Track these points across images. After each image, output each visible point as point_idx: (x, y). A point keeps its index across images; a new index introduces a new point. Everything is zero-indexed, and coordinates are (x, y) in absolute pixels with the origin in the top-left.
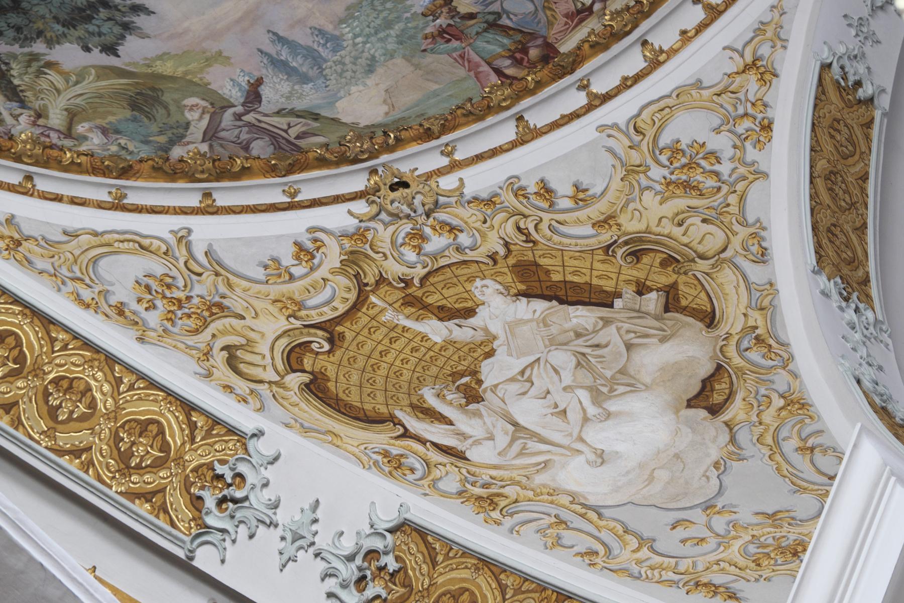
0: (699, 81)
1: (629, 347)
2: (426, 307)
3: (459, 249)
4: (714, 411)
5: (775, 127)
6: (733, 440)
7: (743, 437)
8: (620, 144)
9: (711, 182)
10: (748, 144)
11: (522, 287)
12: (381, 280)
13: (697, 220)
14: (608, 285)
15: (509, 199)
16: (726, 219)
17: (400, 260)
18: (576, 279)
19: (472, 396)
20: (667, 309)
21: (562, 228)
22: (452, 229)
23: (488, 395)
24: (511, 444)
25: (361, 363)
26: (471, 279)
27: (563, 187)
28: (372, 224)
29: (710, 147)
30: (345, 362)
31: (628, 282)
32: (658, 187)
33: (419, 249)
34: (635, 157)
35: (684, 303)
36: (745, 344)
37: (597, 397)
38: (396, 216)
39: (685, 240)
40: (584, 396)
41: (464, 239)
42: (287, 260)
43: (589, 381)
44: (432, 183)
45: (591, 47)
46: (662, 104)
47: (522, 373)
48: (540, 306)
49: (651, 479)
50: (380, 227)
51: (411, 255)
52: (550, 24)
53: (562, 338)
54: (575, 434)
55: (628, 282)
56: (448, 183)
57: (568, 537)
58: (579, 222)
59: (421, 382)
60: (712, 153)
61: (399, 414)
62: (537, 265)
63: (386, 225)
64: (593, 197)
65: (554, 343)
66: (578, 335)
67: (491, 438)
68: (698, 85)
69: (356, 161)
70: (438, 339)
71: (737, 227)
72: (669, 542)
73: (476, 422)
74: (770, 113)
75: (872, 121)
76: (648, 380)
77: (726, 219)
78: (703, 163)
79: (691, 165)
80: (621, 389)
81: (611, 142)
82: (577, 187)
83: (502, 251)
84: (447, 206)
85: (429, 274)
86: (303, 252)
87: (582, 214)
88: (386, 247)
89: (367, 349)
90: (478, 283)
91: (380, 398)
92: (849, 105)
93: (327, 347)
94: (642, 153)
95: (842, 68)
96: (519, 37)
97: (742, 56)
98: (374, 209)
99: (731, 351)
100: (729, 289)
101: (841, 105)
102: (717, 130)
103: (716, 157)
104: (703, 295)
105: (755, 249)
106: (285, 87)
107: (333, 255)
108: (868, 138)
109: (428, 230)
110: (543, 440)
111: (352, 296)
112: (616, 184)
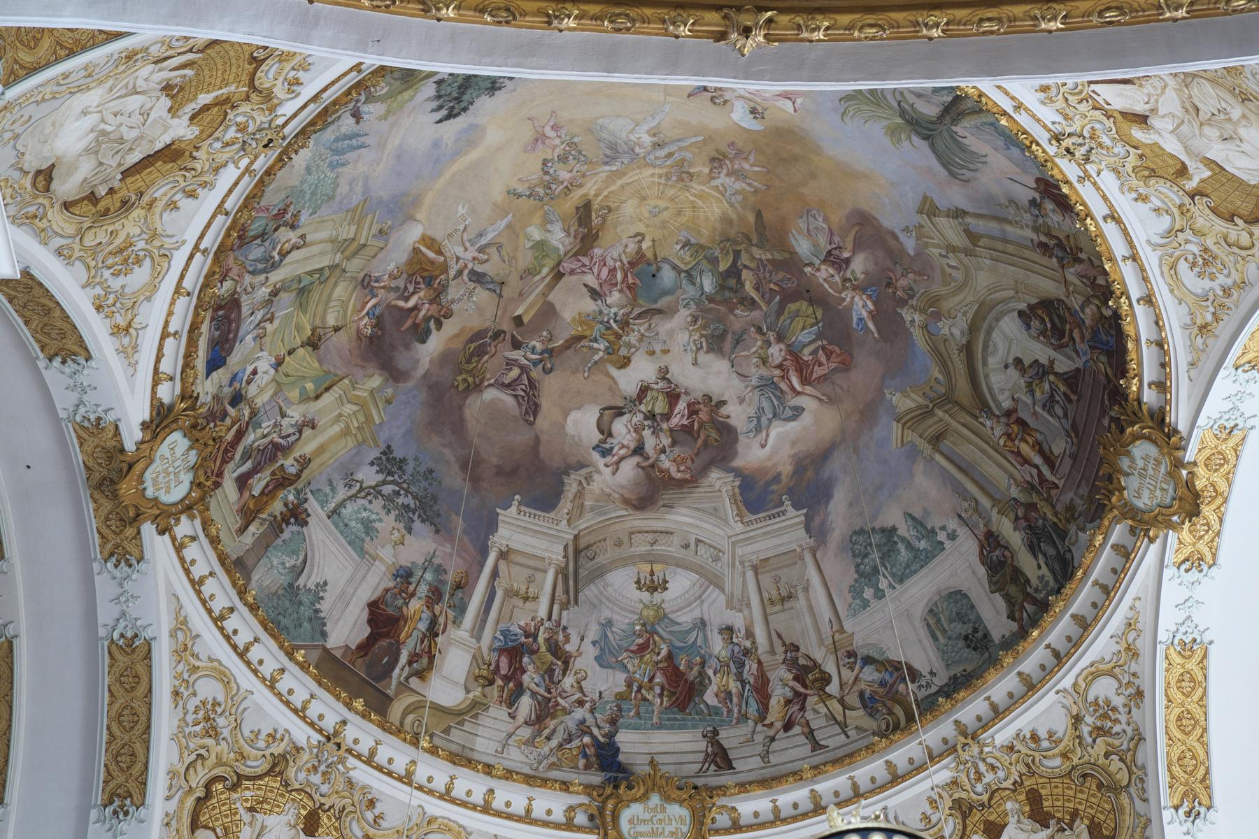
0: (149, 301)
1: (101, 164)
2: (216, 105)
3: (218, 139)
4: (39, 172)
5: (95, 311)
6: (21, 169)
7: (17, 174)
8: (168, 243)
9: (110, 262)
10: (103, 293)
11: (173, 147)
12: (247, 99)
13: (104, 241)
14: (129, 180)
15: (207, 178)
16: (89, 253)
17: (244, 114)
18: (148, 170)
19: (167, 88)
20: (92, 193)
21: (172, 185)
22: (227, 145)
23: (159, 94)
24: (134, 84)
25: (233, 61)
26: (202, 132)
27: (185, 203)
28: (270, 118)
29: (122, 277)
30: (242, 56)
31: (121, 189)
32: (135, 239)
33: (237, 124)
34: (157, 243)
35: (85, 202)
36: (41, 210)
37: (104, 133)
38: (260, 130)
39: (104, 228)
40: (109, 128)
41: (218, 145)
42: (301, 75)
43: (111, 137)
44: (252, 157)
45: (214, 272)
46: (161, 276)
47: (148, 115)
48: (159, 146)
49: (53, 124)
50: (264, 120)
51: (240, 119)
52: (236, 259)
53: (138, 142)
54: (104, 112)
55: (121, 189)
56: (244, 163)
57: (83, 73)
58: (165, 194)
59: (197, 74)
60: (118, 275)
61: (200, 55)
62: (174, 161)
63: (262, 123)
64: (165, 211)
65: (142, 137)
66: (131, 149)
67: (146, 80)
68: (148, 299)
69: (296, 136)
70: (200, 96)
71: (82, 253)
72: (31, 110)
73: (158, 80)
74: (102, 315)
75: (42, 351)
76: (81, 158)
77: (89, 253)
78: (120, 267)
79: (126, 260)
80: (93, 145)
81: (174, 240)
82: (177, 208)
83: (195, 154)
84: (238, 152)
85: (225, 119)
86: (298, 82)
87: (165, 199)
88: (255, 114)
89: (234, 69)
90: (197, 133)
91: (214, 55)
92: (61, 349)
93: (255, 54)
94: (155, 248)
95: (79, 364)
96: (247, 241)
97: (136, 329)
98: (273, 125)
99: (46, 202)
100: (66, 226)
101: (66, 346)
102: (123, 287)
103: (116, 275)
104: (78, 213)
105: (65, 252)
106: (343, 130)
107: (279, 92)
108: (38, 341)
109: (239, 135)
110: (120, 97)
111: (257, 83)
112: (158, 225)
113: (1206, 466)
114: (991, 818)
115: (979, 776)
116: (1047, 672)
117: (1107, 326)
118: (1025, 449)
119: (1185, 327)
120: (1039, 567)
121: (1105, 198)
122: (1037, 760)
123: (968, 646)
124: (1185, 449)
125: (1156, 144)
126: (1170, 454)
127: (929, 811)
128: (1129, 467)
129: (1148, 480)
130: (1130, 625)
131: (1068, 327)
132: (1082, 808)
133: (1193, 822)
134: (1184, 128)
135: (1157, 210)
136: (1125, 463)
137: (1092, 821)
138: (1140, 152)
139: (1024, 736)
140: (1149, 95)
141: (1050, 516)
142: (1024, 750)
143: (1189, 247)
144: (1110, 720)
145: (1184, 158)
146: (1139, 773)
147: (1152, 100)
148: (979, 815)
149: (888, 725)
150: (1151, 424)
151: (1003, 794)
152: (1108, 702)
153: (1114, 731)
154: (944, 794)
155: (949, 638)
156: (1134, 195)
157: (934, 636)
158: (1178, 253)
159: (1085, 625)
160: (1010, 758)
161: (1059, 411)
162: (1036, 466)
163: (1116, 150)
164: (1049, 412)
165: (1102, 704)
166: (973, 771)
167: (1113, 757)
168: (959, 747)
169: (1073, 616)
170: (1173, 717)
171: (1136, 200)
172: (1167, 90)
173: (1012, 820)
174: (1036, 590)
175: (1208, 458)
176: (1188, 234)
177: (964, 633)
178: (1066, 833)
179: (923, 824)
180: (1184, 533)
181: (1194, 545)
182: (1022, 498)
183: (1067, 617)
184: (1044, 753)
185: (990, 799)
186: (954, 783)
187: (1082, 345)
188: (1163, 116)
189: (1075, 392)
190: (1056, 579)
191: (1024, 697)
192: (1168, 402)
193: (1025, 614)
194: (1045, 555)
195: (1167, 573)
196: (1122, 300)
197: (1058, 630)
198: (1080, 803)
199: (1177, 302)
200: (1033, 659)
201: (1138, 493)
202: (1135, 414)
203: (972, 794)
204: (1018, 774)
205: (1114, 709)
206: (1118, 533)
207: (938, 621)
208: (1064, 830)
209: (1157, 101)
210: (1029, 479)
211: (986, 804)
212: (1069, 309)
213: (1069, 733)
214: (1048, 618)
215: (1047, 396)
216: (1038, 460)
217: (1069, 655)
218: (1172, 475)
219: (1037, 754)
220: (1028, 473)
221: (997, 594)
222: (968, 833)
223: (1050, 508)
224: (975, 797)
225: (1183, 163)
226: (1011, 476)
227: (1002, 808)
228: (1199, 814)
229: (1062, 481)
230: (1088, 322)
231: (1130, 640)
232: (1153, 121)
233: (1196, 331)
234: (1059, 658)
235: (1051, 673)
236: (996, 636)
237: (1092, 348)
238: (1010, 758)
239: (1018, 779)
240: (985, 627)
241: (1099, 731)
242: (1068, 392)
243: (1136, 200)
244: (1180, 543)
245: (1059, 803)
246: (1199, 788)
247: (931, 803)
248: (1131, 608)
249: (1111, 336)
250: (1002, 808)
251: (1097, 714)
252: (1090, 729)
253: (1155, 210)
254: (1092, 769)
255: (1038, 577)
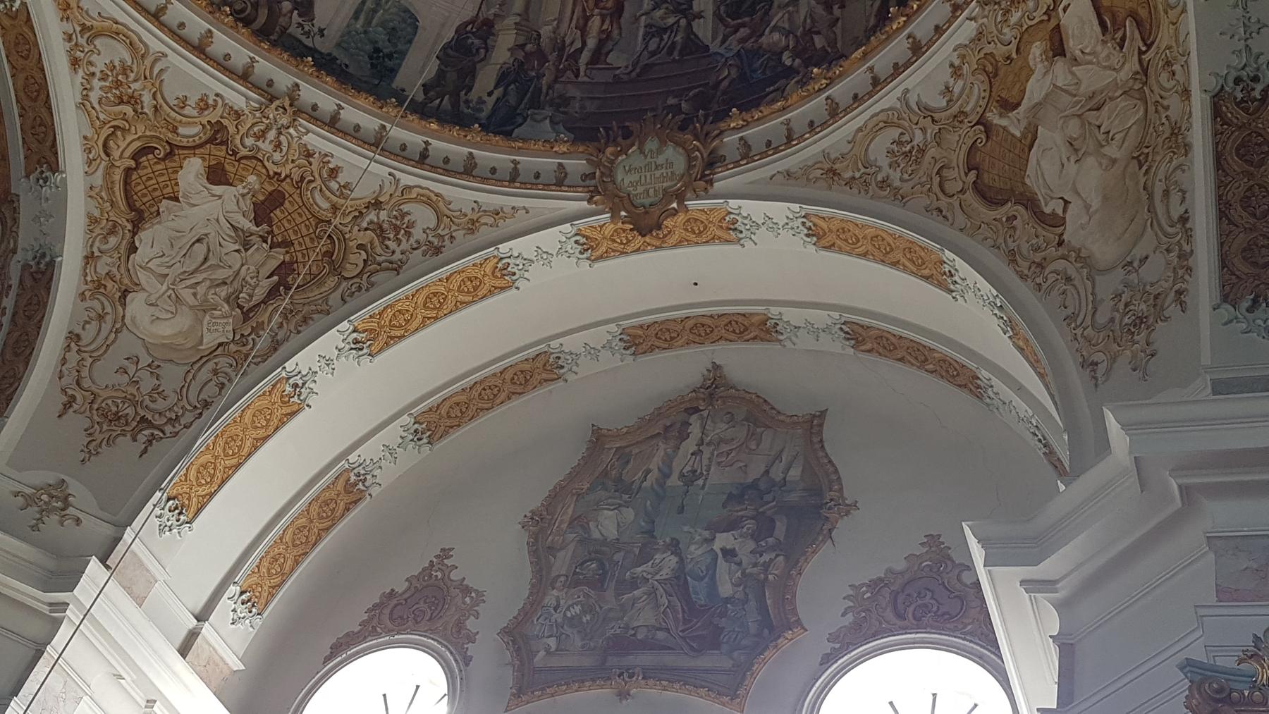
113: (688, 220)
114: (227, 166)
115: (261, 136)
116: (401, 153)
117: (772, 63)
118: (595, 23)
119: (825, 154)
120: (490, 94)
121: (939, 30)
122: (313, 185)
123: (371, 58)
124: (698, 198)
125: (1031, 72)
126: (686, 185)
127: (192, 102)
128: (651, 151)
129: (648, 175)
130: (497, 214)
131: (747, 19)
132: (297, 247)
133: (352, 349)
134: (1066, 99)
135: (948, 89)
136: (651, 144)
137: (291, 263)
138: (1014, 55)
139: (329, 162)
140: (1093, 53)
141: (544, 81)
142: (314, 167)
143: (918, 133)
144: (395, 235)
145: (1025, 104)
146: (364, 283)
147: (1088, 58)
148: (223, 154)
149: (243, 11)
150: (705, 155)
151: (259, 168)
152: (411, 225)
153: (387, 242)
154: (219, 110)
155: (365, 32)
156: (957, 63)
157: (356, 16)
158: (906, 124)
159: (469, 170)
160: (298, 159)
161: (653, 45)
162: (584, 44)
163: (1006, 30)
164: (646, 34)
165: (406, 220)
166: (262, 128)
167: (363, 252)
168: (277, 103)
169: (471, 154)
170: (433, 289)
171: (952, 65)
172: (1109, 72)
173: (240, 189)
174: (467, 102)
175: (696, 220)
176: (932, 130)
177: (380, 45)
178: (264, 245)
179: (176, 102)
180: (612, 226)
181: (604, 238)
182: (545, 41)
183: (466, 150)
184: (324, 188)
185: (245, 157)
186: (238, 115)
187: (735, 43)
188: (1072, 73)
189: (681, 54)
190: (489, 118)
191: (364, 142)
192: (737, 164)
193: (438, 101)
194: (505, 94)
195: (567, 227)
196: (824, 81)
197: (446, 146)
198: (300, 244)
199: (850, 139)
200: (406, 134)
201: (630, 170)
202: (707, 134)
203: (238, 137)
204: (288, 172)
205: (408, 234)
206: (576, 165)
207: (375, 11)
208: (267, 243)
209: (1090, 63)
210: (568, 42)
211: (238, 156)
212: (767, 13)
213: (358, 202)
214: (456, 131)
215: (662, 24)
216: (591, 43)
217: (433, 168)
218: (668, 195)
219: (319, 182)
220: (572, 36)
221: (438, 62)
222: (197, 151)
223: (552, 77)
224: (238, 141)
225: (1018, 104)
226: (560, 21)
227: (244, 173)
228: (362, 349)
229: (586, 79)
230: (764, 40)
231: (483, 220)
232: (1060, 65)
233: (826, 166)
234: (423, 159)
235: (407, 160)
236: (399, 81)
237: (738, 54)
238: (298, 159)
239: (283, 176)
240: (400, 65)
241: (379, 229)
242: (679, 47)
243: (952, 65)
244: (601, 227)
245: (286, 225)
246: (383, 338)
247: (201, 100)
248: (513, 208)
249: (764, 73)
250: (244, 173)
251: (393, 220)
252: (376, 220)
253: (947, 88)
254: (338, 239)
255: (480, 98)
